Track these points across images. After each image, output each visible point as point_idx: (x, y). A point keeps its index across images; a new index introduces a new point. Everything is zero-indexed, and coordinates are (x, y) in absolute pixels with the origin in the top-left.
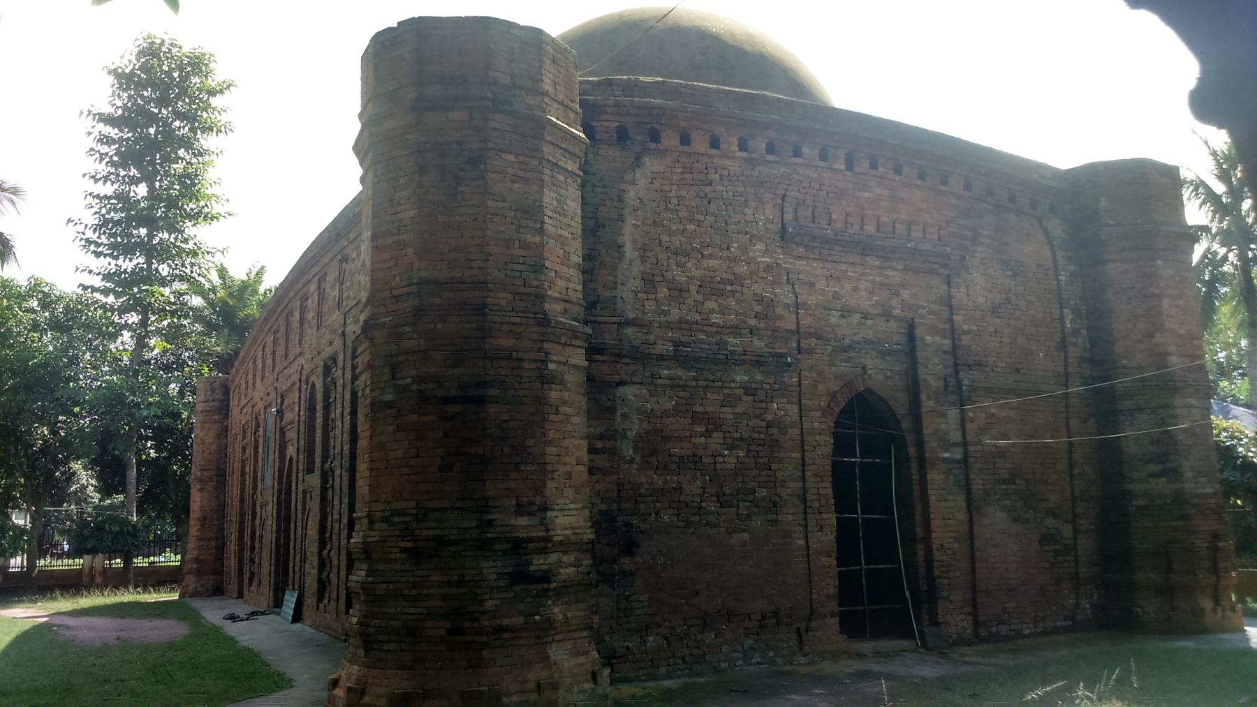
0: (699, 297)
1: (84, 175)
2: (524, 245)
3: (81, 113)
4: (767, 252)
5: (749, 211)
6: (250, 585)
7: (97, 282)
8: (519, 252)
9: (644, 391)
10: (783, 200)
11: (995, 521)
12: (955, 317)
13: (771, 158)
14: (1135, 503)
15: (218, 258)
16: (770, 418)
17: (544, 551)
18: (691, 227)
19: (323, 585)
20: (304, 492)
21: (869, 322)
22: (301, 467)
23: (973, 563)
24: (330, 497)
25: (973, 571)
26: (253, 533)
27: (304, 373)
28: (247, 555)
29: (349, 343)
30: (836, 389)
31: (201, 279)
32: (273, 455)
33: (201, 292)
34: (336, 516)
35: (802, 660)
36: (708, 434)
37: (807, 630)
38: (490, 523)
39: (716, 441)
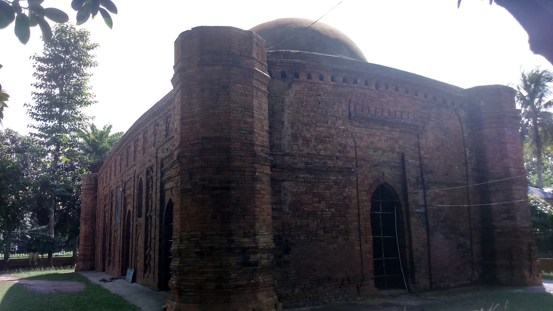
0: (315, 144)
1: (32, 85)
2: (246, 122)
3: (30, 57)
4: (343, 124)
5: (336, 107)
6: (109, 266)
7: (36, 131)
8: (243, 126)
9: (293, 184)
10: (350, 102)
11: (439, 238)
12: (422, 152)
13: (344, 84)
14: (496, 231)
15: (91, 122)
16: (345, 195)
17: (255, 253)
18: (312, 114)
19: (146, 267)
20: (137, 226)
21: (386, 154)
22: (135, 214)
23: (430, 256)
24: (149, 228)
25: (430, 259)
26: (110, 243)
27: (137, 174)
28: (107, 253)
29: (159, 161)
31: (83, 130)
32: (121, 208)
33: (83, 136)
34: (153, 236)
35: (359, 298)
36: (319, 202)
37: (361, 286)
38: (233, 241)
39: (323, 205)
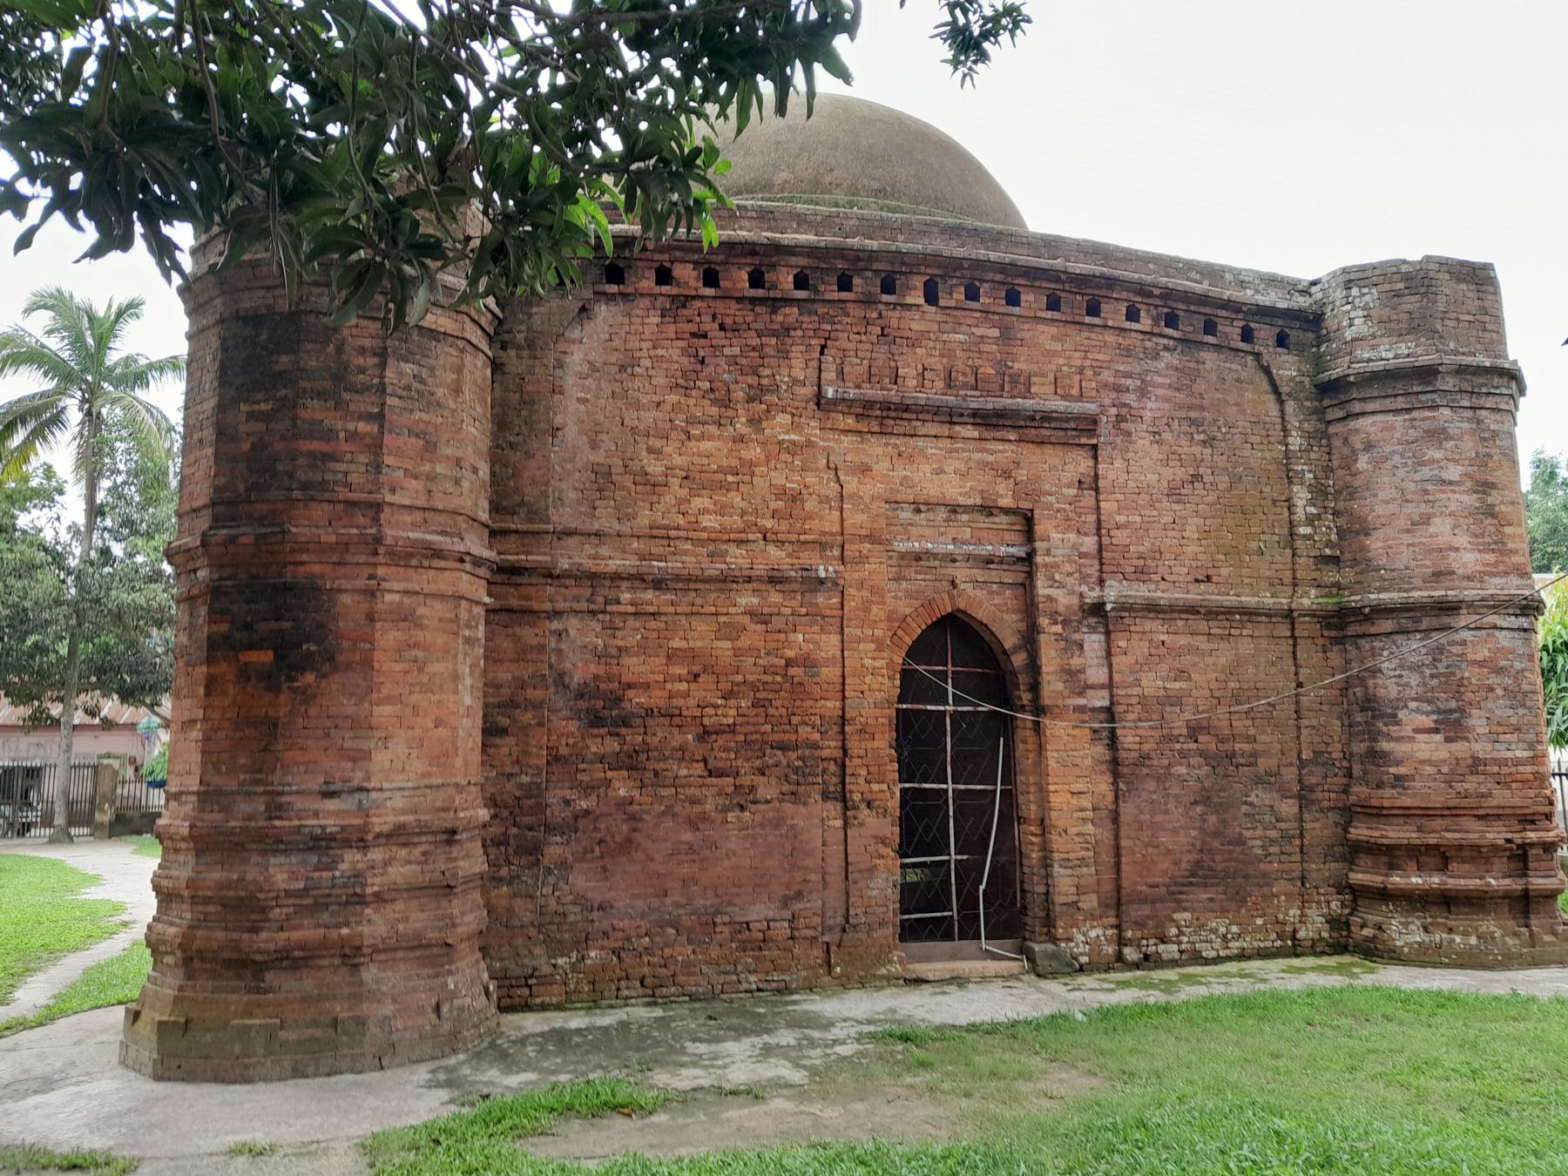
0: (684, 493)
4: (794, 427)
14: (1392, 770)
16: (790, 654)
23: (1118, 855)
30: (908, 611)
